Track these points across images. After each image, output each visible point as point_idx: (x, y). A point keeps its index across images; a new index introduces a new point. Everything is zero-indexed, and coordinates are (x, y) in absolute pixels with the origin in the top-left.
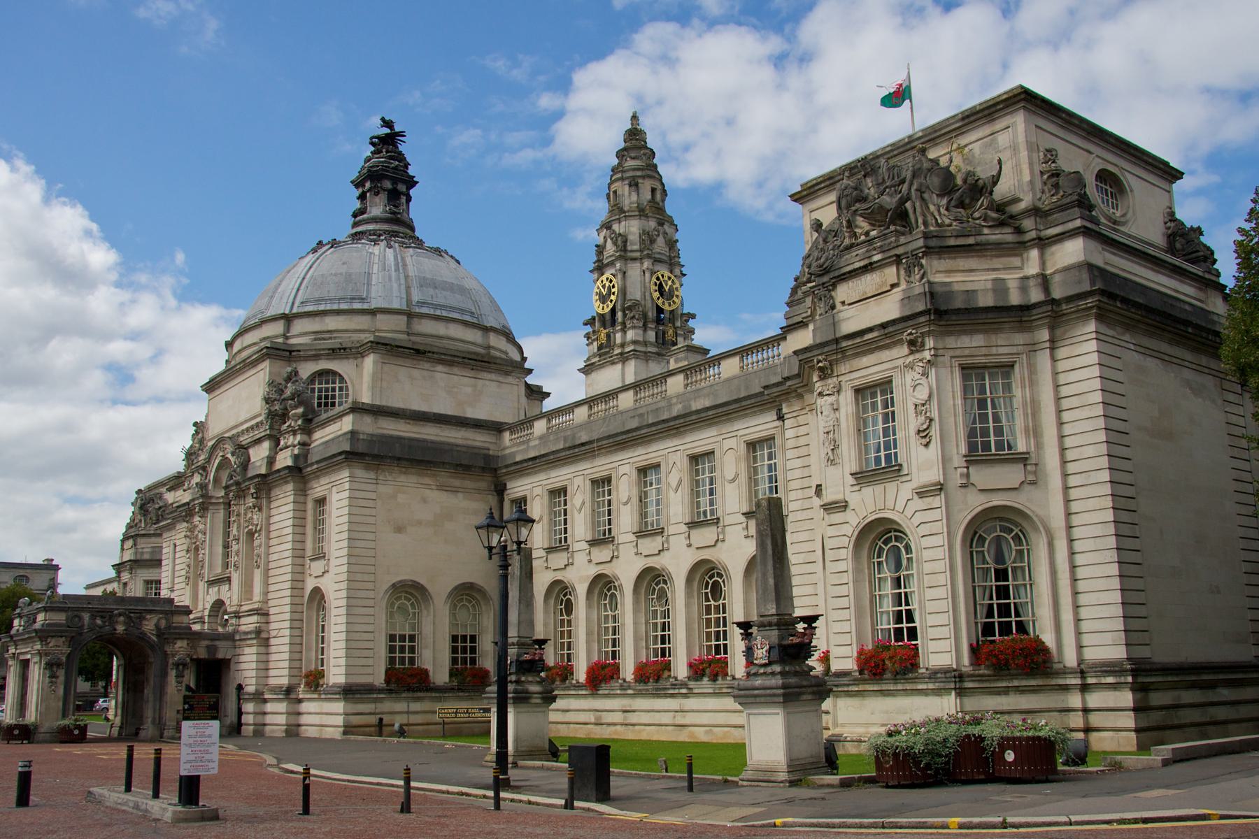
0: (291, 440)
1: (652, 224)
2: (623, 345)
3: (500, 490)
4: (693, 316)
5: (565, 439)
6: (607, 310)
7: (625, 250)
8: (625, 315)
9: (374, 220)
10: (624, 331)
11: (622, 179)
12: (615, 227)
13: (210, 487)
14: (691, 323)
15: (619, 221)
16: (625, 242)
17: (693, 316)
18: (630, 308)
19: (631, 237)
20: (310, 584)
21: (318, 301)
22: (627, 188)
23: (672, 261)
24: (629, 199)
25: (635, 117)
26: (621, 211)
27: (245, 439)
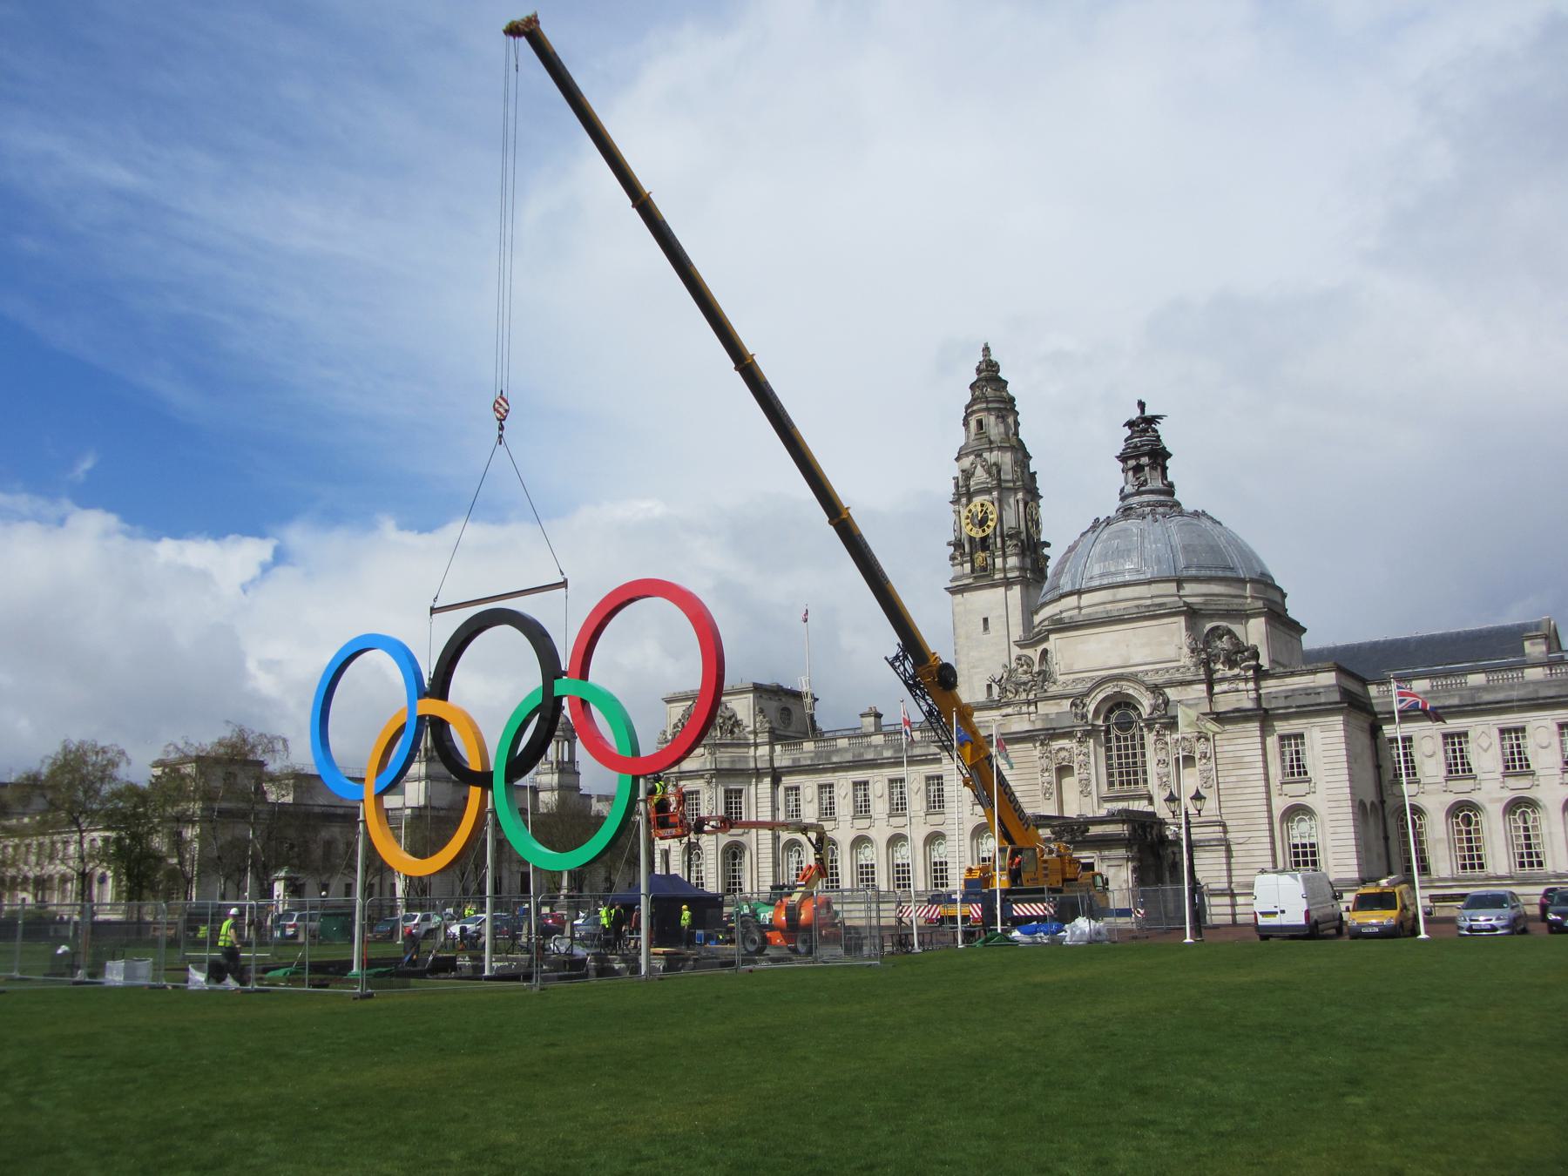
0: (1242, 686)
1: (1020, 456)
2: (1004, 570)
3: (1375, 730)
4: (1048, 545)
5: (1461, 697)
6: (981, 534)
7: (1000, 480)
8: (1003, 542)
9: (1152, 492)
10: (1004, 556)
11: (988, 410)
12: (986, 455)
13: (1090, 716)
14: (1046, 551)
15: (991, 450)
16: (999, 472)
17: (1048, 545)
18: (1011, 537)
20: (1280, 804)
21: (1199, 567)
22: (992, 418)
23: (1033, 494)
24: (994, 429)
25: (986, 349)
26: (991, 442)
27: (1153, 679)
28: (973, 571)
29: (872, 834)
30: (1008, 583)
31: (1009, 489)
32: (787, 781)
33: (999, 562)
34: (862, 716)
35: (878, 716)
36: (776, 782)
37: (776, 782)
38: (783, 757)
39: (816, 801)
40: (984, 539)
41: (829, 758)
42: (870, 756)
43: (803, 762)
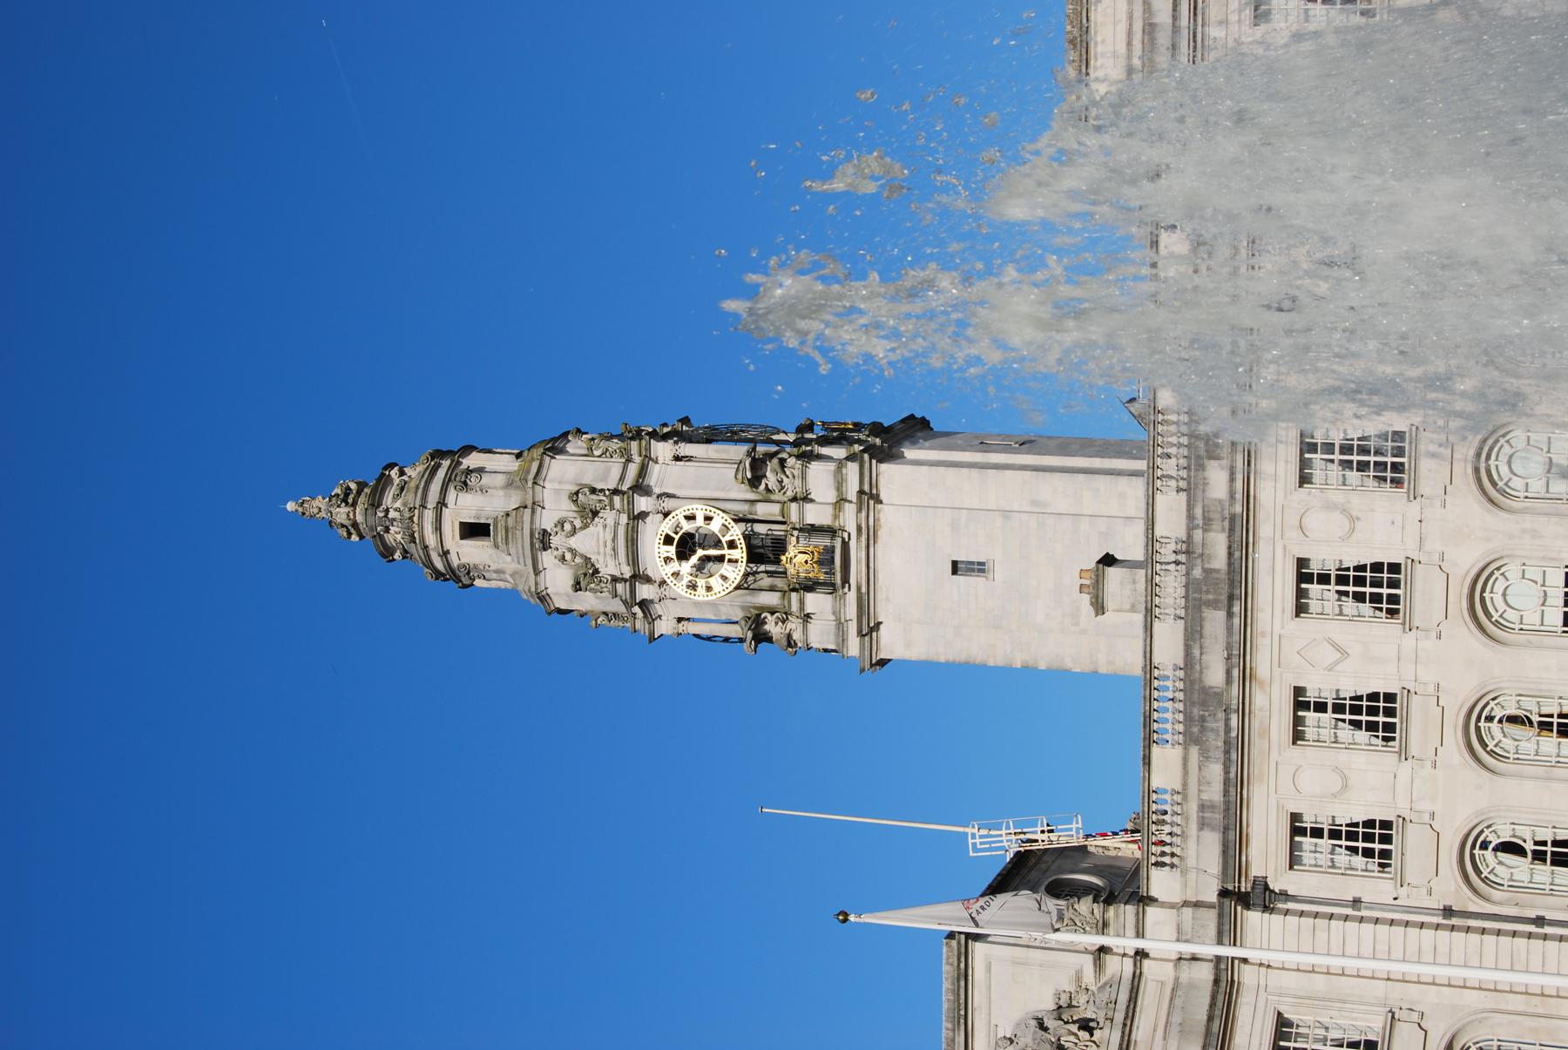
6: (740, 554)
12: (547, 521)
19: (588, 480)
28: (831, 587)
29: (1465, 562)
30: (869, 496)
31: (643, 471)
32: (1265, 855)
33: (816, 515)
34: (1099, 608)
35: (1108, 560)
36: (1263, 897)
37: (1263, 897)
38: (1186, 877)
39: (1343, 757)
40: (754, 556)
41: (1205, 691)
42: (1218, 545)
43: (1215, 793)
